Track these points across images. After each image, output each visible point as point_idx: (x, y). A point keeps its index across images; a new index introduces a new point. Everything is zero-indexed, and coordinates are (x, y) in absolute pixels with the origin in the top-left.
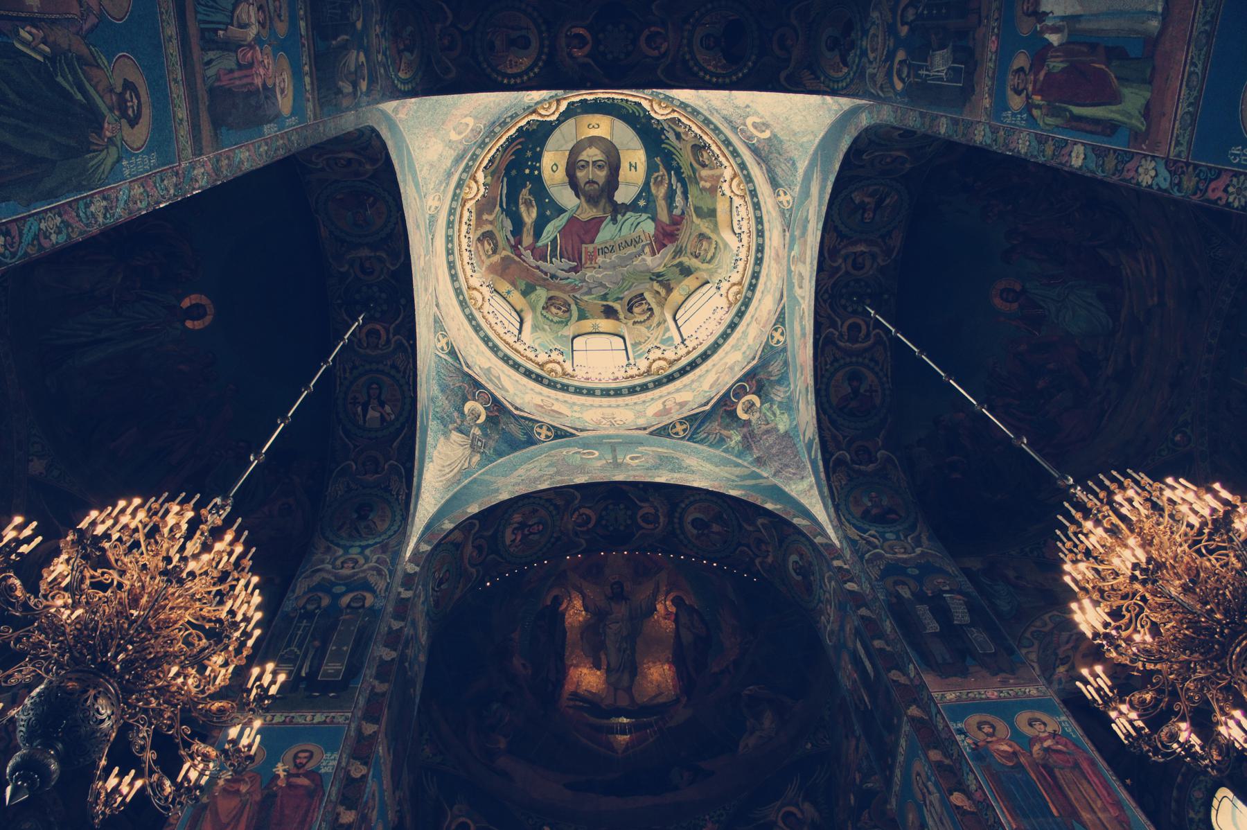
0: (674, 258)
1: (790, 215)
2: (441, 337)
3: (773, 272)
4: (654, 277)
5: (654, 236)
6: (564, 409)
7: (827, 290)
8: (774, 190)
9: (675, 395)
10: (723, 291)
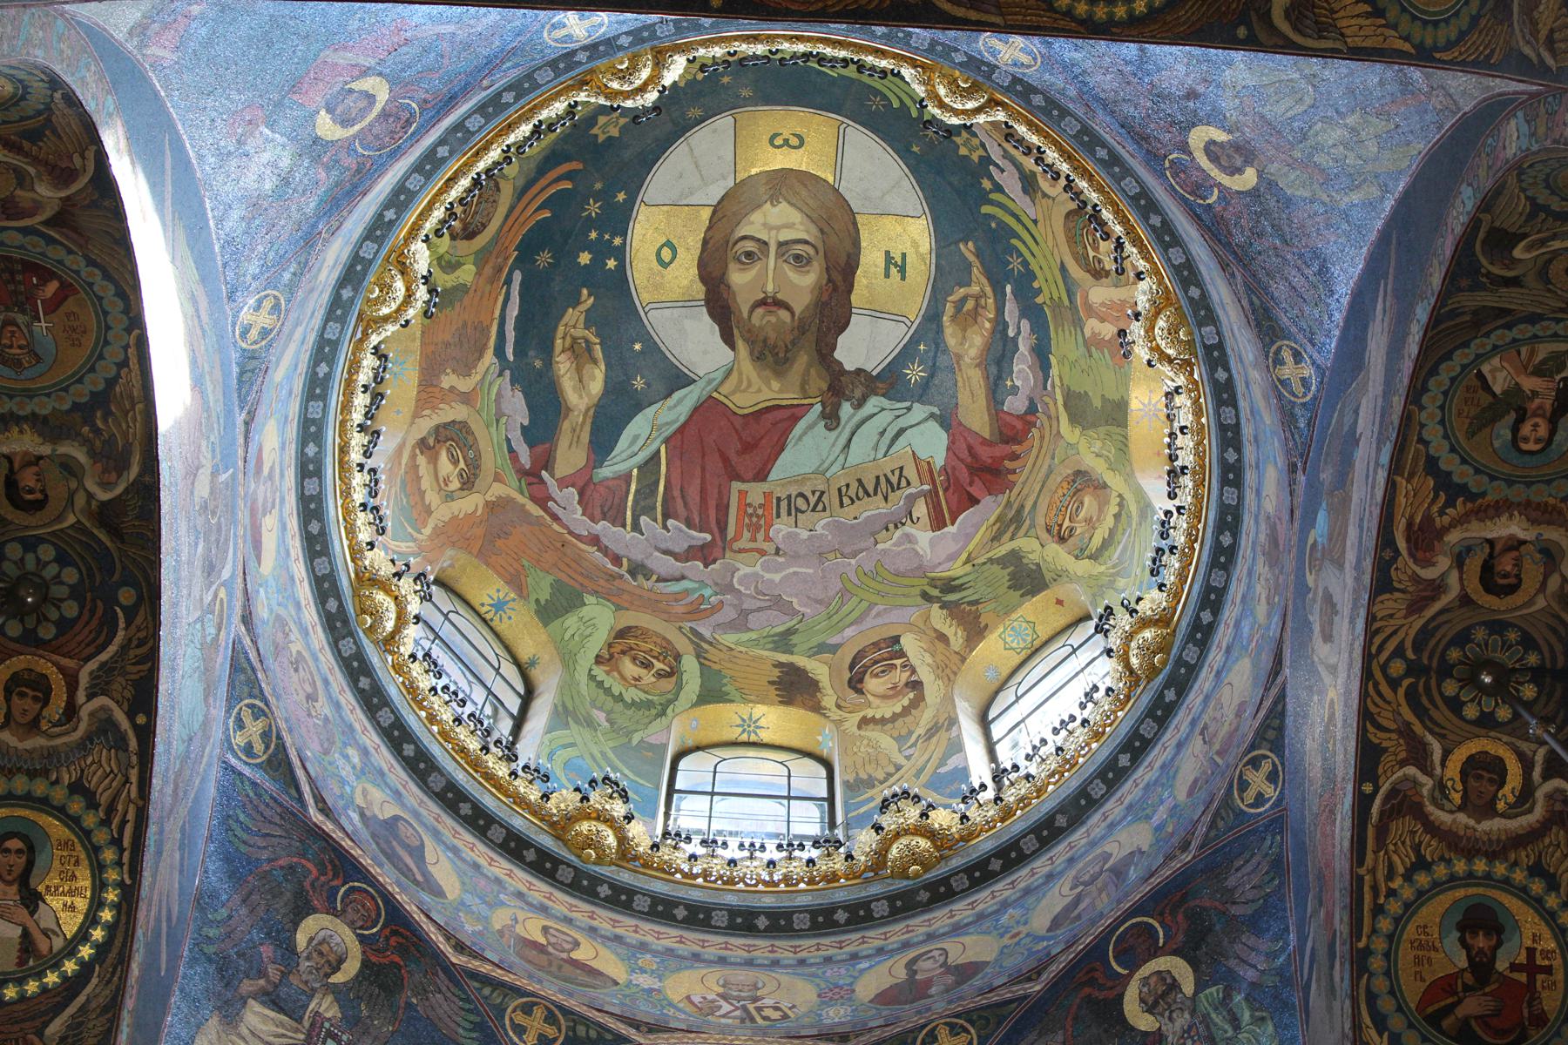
0: (996, 538)
1: (1310, 424)
2: (247, 717)
3: (1260, 589)
4: (935, 592)
5: (944, 468)
6: (609, 963)
7: (1399, 652)
10: (1114, 641)
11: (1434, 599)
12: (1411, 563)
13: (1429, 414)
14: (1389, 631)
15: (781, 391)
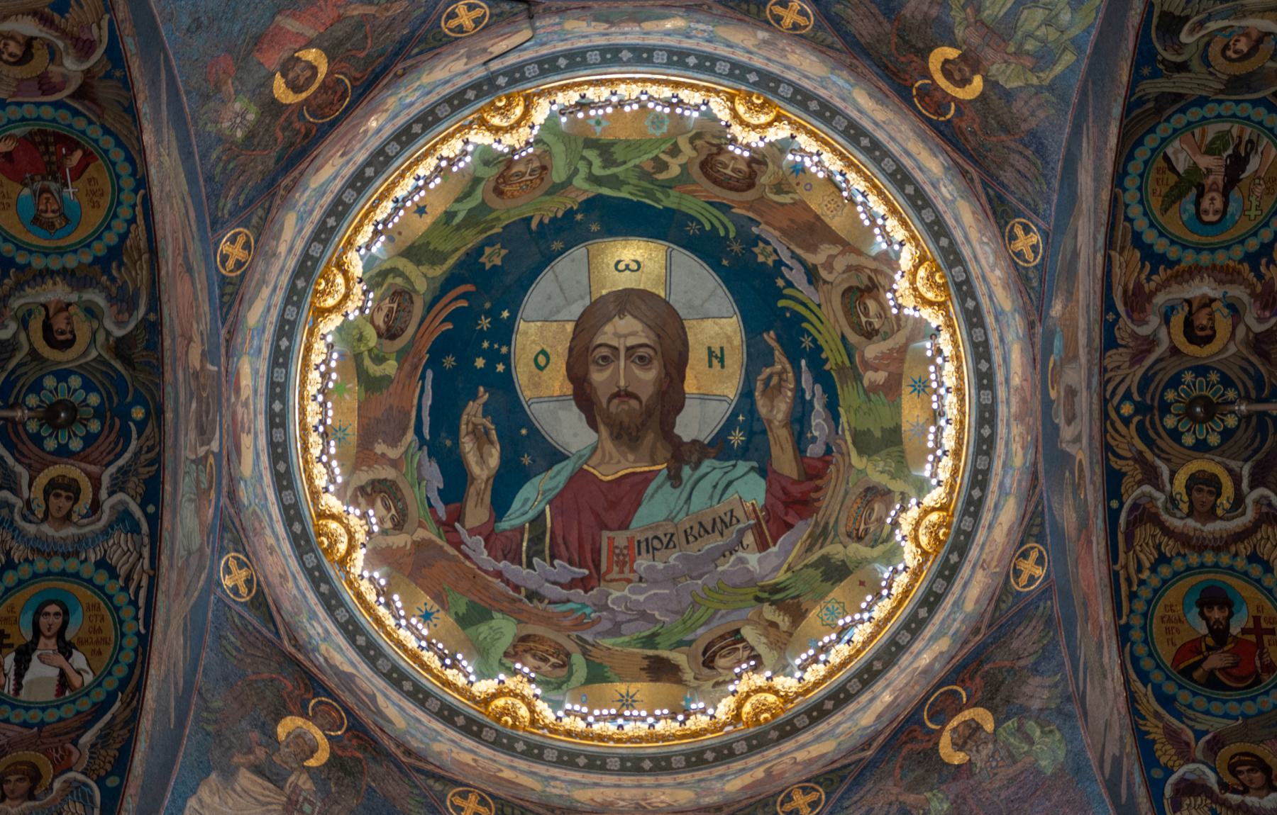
0: (809, 550)
1: (1041, 281)
3: (1016, 447)
4: (766, 595)
5: (765, 507)
7: (1127, 396)
8: (1001, 228)
9: (795, 755)
11: (1149, 351)
12: (1129, 323)
13: (1131, 196)
14: (1118, 379)
15: (635, 461)
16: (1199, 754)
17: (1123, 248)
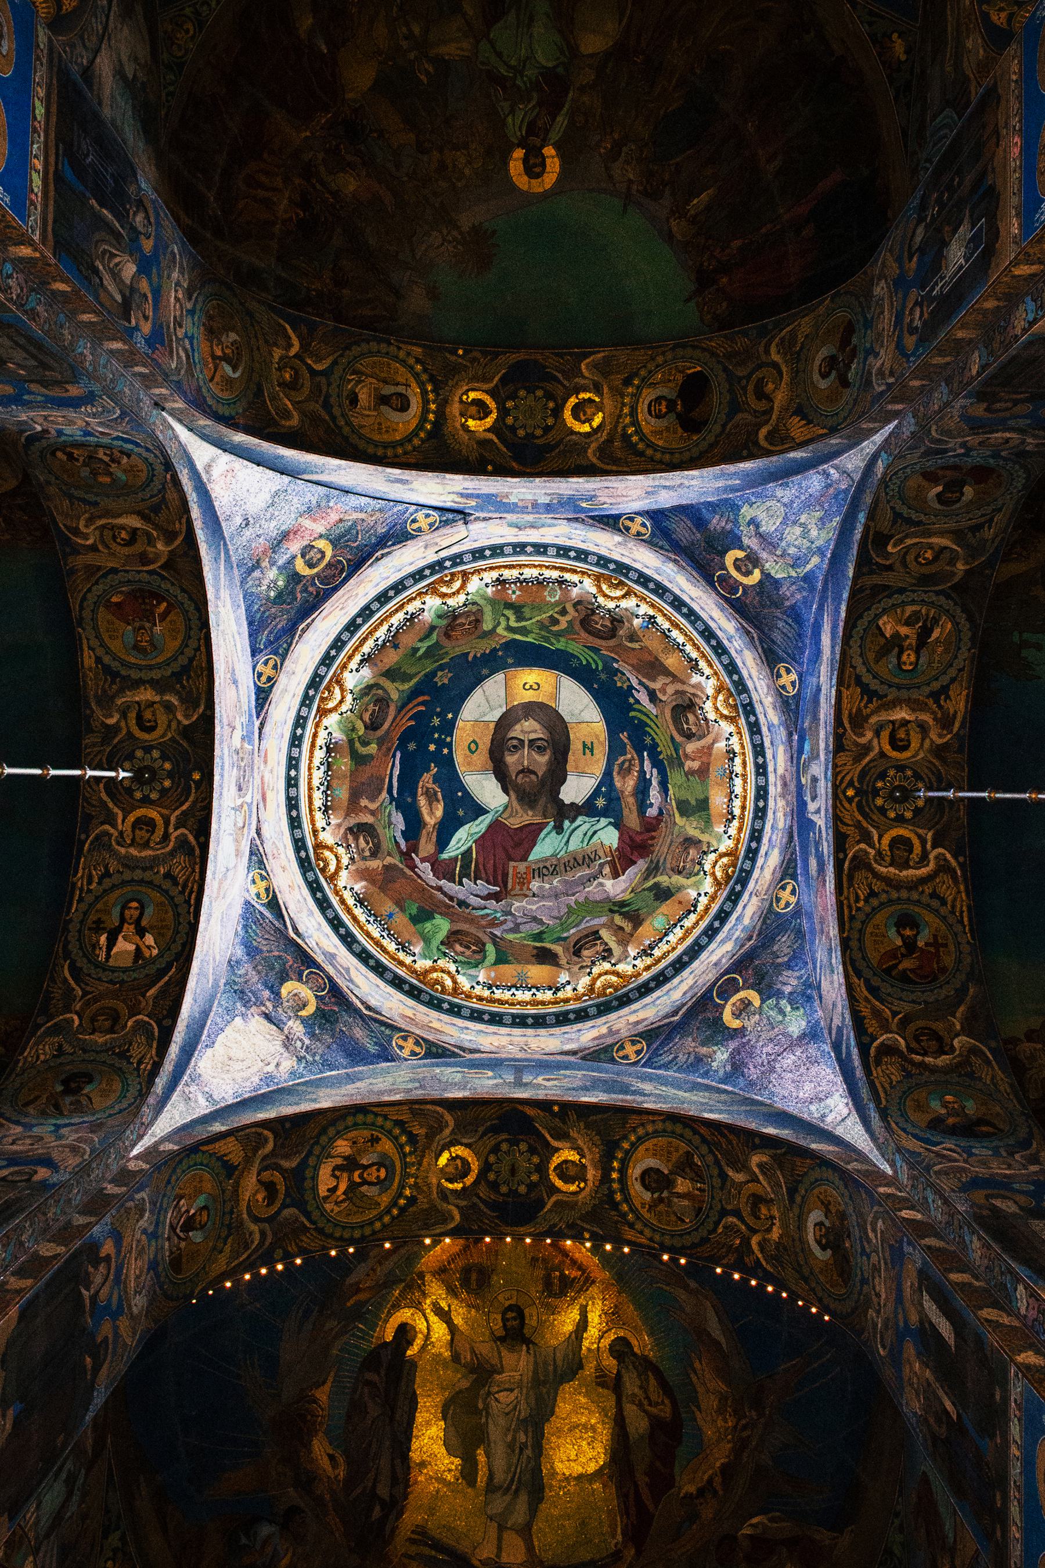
3: (780, 815)
5: (617, 849)
7: (851, 784)
11: (866, 754)
16: (894, 1027)
17: (849, 686)
